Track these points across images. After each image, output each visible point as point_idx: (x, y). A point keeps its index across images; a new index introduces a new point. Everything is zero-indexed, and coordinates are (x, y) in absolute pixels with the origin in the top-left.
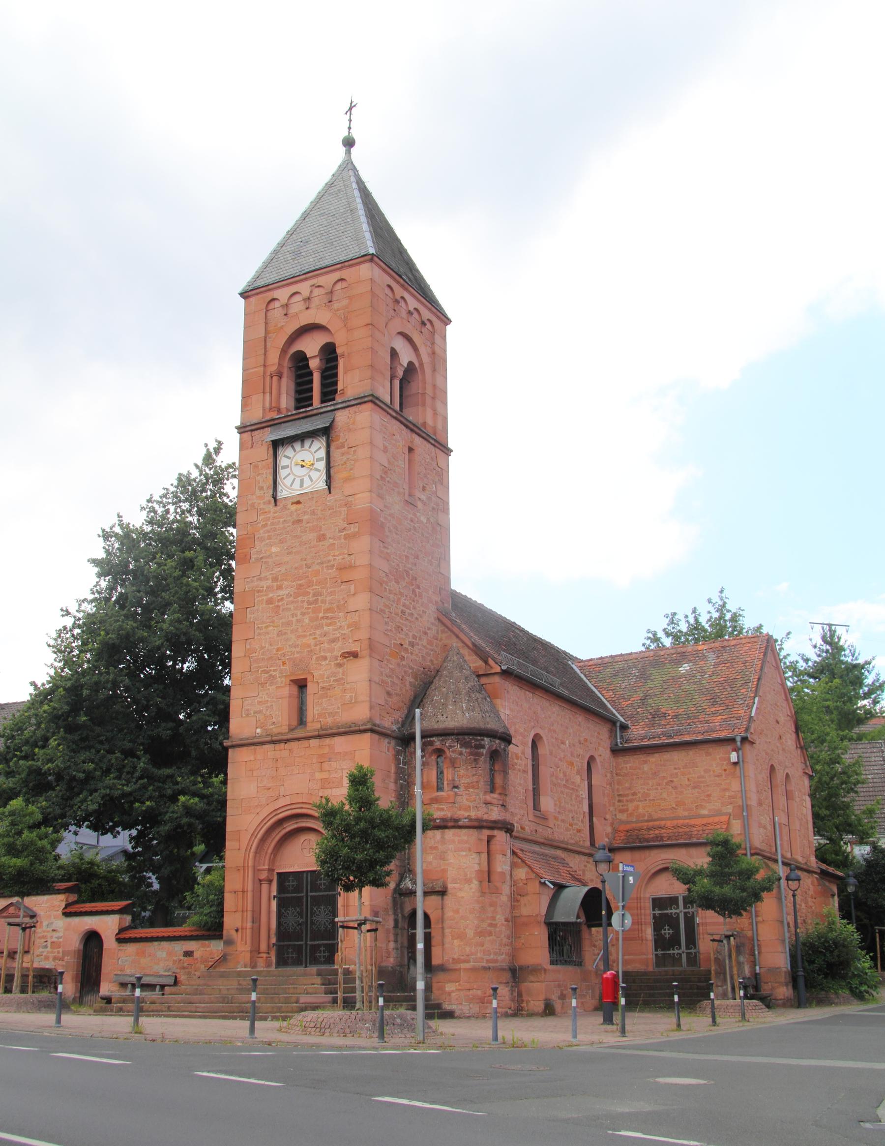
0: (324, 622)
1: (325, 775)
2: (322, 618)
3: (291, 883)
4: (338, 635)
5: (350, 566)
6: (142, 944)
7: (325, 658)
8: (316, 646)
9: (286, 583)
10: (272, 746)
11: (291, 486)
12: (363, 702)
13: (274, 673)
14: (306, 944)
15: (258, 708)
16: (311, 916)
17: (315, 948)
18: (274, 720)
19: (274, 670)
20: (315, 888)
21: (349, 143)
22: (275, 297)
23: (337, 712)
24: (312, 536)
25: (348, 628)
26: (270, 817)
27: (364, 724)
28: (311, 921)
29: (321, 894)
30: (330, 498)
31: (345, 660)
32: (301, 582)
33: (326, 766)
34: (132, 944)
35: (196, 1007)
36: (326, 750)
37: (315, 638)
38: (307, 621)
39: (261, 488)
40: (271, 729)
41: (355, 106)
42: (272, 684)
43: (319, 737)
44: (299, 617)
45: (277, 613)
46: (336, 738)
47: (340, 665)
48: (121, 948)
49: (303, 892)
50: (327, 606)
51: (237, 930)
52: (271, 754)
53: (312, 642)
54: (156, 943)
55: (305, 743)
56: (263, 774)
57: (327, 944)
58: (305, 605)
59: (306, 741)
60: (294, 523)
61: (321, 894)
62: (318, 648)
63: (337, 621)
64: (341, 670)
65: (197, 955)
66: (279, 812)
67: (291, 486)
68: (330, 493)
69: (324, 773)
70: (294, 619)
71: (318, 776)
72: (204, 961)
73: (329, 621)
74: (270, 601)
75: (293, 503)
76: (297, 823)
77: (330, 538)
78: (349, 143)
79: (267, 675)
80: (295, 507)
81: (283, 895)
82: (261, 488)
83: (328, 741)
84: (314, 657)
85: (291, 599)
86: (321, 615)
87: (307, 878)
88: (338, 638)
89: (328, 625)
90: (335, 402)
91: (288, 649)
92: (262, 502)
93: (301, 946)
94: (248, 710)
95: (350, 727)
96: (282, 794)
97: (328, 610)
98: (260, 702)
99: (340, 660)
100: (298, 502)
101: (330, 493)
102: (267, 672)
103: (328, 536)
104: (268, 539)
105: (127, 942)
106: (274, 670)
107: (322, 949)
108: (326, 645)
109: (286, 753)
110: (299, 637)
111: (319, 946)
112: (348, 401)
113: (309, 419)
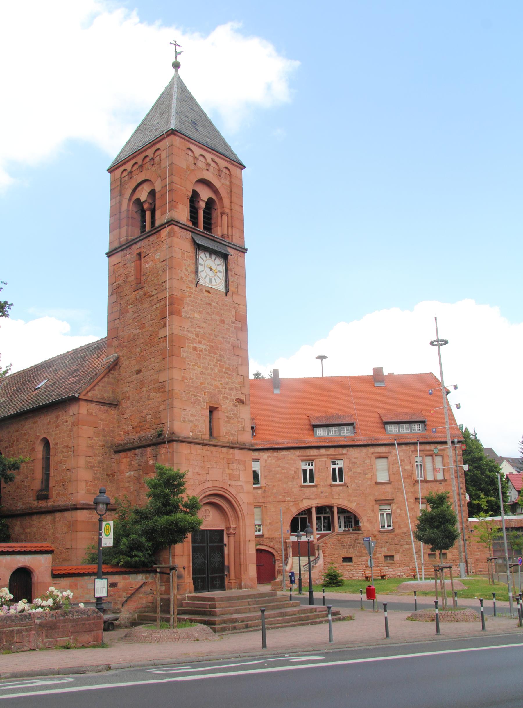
0: (226, 375)
1: (230, 472)
2: (225, 372)
3: (198, 537)
4: (233, 387)
5: (238, 347)
6: (74, 578)
7: (228, 399)
8: (222, 389)
9: (204, 341)
11: (216, 283)
12: (248, 432)
13: (200, 398)
14: (208, 576)
15: (191, 418)
16: (210, 559)
17: (213, 579)
18: (200, 429)
19: (200, 396)
20: (212, 541)
21: (176, 66)
23: (235, 434)
25: (238, 384)
26: (231, 496)
27: (248, 446)
28: (210, 561)
30: (225, 298)
31: (238, 403)
33: (231, 466)
34: (65, 579)
35: (278, 620)
36: (231, 457)
37: (221, 384)
38: (217, 371)
40: (199, 435)
41: (175, 42)
42: (198, 405)
43: (228, 447)
44: (212, 367)
45: (199, 358)
46: (235, 450)
47: (236, 406)
48: (55, 582)
49: (205, 543)
50: (227, 366)
51: (184, 568)
52: (200, 451)
53: (220, 386)
54: (86, 578)
55: (220, 449)
56: (196, 464)
57: (219, 576)
59: (220, 448)
60: (207, 304)
62: (223, 390)
63: (233, 377)
64: (236, 408)
65: (120, 585)
66: (228, 493)
67: (216, 283)
68: (226, 296)
69: (230, 470)
70: (209, 367)
72: (125, 590)
74: (195, 349)
75: (206, 291)
76: (209, 499)
77: (227, 324)
78: (176, 66)
79: (195, 398)
80: (206, 294)
81: (221, 544)
82: (187, 270)
83: (231, 451)
84: (222, 395)
85: (207, 353)
86: (224, 370)
87: (207, 533)
88: (234, 388)
89: (229, 378)
91: (207, 385)
93: (205, 577)
94: (184, 418)
95: (246, 445)
96: (208, 480)
97: (228, 369)
98: (192, 415)
99: (235, 402)
100: (209, 292)
101: (226, 296)
102: (195, 396)
103: (226, 322)
104: (192, 307)
105: (61, 577)
106: (200, 396)
107: (217, 579)
108: (227, 390)
109: (208, 453)
110: (213, 379)
111: (215, 577)
112: (236, 246)
113: (213, 242)
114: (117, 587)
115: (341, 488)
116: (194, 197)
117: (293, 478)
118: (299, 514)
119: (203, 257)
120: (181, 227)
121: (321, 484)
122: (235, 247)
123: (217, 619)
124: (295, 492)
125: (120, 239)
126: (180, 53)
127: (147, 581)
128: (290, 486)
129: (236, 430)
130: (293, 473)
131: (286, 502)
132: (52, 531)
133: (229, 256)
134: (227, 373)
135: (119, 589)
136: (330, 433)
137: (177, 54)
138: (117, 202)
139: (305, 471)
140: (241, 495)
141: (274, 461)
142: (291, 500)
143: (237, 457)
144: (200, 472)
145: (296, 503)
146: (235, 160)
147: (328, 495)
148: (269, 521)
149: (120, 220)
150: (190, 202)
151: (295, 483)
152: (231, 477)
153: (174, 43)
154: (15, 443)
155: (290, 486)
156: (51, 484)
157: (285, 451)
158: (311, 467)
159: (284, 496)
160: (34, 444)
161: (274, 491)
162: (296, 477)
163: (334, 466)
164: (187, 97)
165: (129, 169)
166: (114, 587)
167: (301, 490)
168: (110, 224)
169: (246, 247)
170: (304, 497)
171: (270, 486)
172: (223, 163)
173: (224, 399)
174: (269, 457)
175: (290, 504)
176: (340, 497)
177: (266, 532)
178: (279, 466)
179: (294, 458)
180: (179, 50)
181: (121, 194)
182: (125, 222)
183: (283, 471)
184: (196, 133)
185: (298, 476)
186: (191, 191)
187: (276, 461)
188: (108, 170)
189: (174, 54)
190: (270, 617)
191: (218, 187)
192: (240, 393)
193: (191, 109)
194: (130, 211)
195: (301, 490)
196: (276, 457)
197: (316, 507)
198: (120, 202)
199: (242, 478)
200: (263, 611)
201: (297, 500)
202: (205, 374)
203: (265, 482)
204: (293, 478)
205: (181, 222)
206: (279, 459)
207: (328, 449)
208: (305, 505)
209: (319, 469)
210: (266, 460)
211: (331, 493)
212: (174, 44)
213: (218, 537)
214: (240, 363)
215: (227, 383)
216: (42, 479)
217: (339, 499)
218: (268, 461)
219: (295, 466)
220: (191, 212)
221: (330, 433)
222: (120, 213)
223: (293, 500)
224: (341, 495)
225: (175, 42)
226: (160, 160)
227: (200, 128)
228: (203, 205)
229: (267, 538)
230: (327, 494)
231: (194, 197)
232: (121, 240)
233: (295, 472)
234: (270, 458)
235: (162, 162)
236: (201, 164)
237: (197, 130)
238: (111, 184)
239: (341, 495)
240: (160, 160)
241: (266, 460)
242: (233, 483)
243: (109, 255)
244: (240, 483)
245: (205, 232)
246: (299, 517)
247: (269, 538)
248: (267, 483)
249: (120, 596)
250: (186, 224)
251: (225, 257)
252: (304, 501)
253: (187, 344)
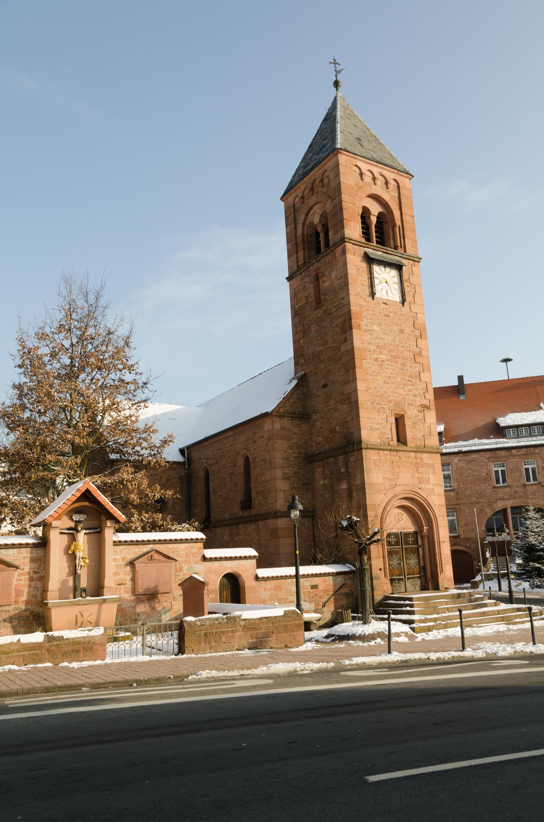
0: (409, 382)
3: (393, 540)
4: (417, 393)
12: (435, 436)
13: (385, 407)
15: (377, 426)
22: (358, 165)
24: (397, 328)
29: (410, 546)
31: (423, 409)
32: (393, 354)
38: (399, 379)
39: (362, 285)
43: (416, 452)
50: (409, 374)
58: (398, 369)
61: (410, 546)
63: (416, 384)
65: (321, 588)
68: (403, 306)
71: (417, 475)
74: (376, 360)
75: (383, 303)
79: (380, 406)
80: (384, 306)
82: (362, 285)
83: (419, 455)
85: (389, 362)
88: (417, 395)
90: (397, 251)
92: (364, 294)
96: (398, 484)
97: (409, 376)
100: (386, 304)
101: (403, 306)
103: (406, 332)
104: (371, 319)
109: (397, 459)
115: (535, 487)
116: (365, 214)
117: (486, 479)
118: (493, 515)
119: (376, 269)
120: (354, 244)
121: (515, 484)
122: (409, 257)
123: (415, 617)
124: (488, 494)
125: (298, 263)
126: (340, 72)
127: (346, 582)
128: (483, 488)
130: (485, 475)
131: (480, 504)
132: (257, 538)
133: (404, 267)
136: (521, 434)
137: (337, 72)
138: (293, 228)
139: (497, 472)
140: (432, 497)
141: (464, 464)
142: (485, 501)
143: (425, 461)
145: (490, 504)
146: (402, 170)
147: (522, 495)
148: (464, 522)
149: (296, 245)
150: (361, 219)
151: (487, 485)
152: (420, 481)
153: (333, 61)
154: (219, 460)
155: (483, 488)
156: (253, 495)
157: (475, 454)
158: (503, 468)
159: (477, 498)
160: (236, 459)
161: (467, 493)
162: (488, 479)
163: (527, 467)
164: (350, 114)
165: (300, 195)
166: (316, 589)
167: (495, 491)
168: (288, 250)
169: (420, 256)
170: (498, 497)
171: (462, 489)
172: (390, 175)
174: (459, 460)
175: (484, 506)
176: (535, 497)
177: (461, 533)
178: (470, 469)
179: (484, 460)
180: (339, 68)
181: (295, 221)
182: (301, 246)
183: (475, 474)
184: (361, 149)
185: (490, 478)
186: (362, 207)
187: (467, 464)
188: (281, 199)
189: (335, 73)
190: (469, 616)
191: (387, 201)
193: (355, 126)
194: (305, 236)
195: (495, 491)
196: (467, 460)
197: (511, 507)
198: (296, 228)
199: (432, 481)
200: (460, 611)
201: (490, 501)
202: (388, 383)
203: (457, 485)
204: (486, 479)
205: (354, 239)
206: (470, 462)
207: (519, 450)
208: (500, 505)
209: (511, 470)
210: (457, 464)
211: (525, 493)
212: (333, 63)
213: (412, 539)
215: (411, 391)
216: (245, 491)
217: (535, 498)
218: (459, 465)
219: (486, 468)
220: (363, 228)
221: (521, 434)
222: (296, 238)
223: (487, 501)
224: (536, 494)
225: (335, 61)
226: (329, 182)
227: (365, 144)
228: (374, 220)
229: (463, 539)
230: (522, 494)
231: (365, 214)
232: (299, 264)
233: (487, 474)
234: (461, 462)
235: (331, 182)
236: (368, 177)
237: (362, 146)
238: (286, 211)
239: (536, 494)
240: (329, 182)
241: (457, 464)
242: (423, 486)
243: (289, 279)
244: (430, 486)
245: (378, 246)
246: (494, 518)
247: (465, 539)
248: (459, 486)
249: (321, 597)
250: (358, 240)
251: (399, 267)
252: (498, 502)
253: (368, 356)
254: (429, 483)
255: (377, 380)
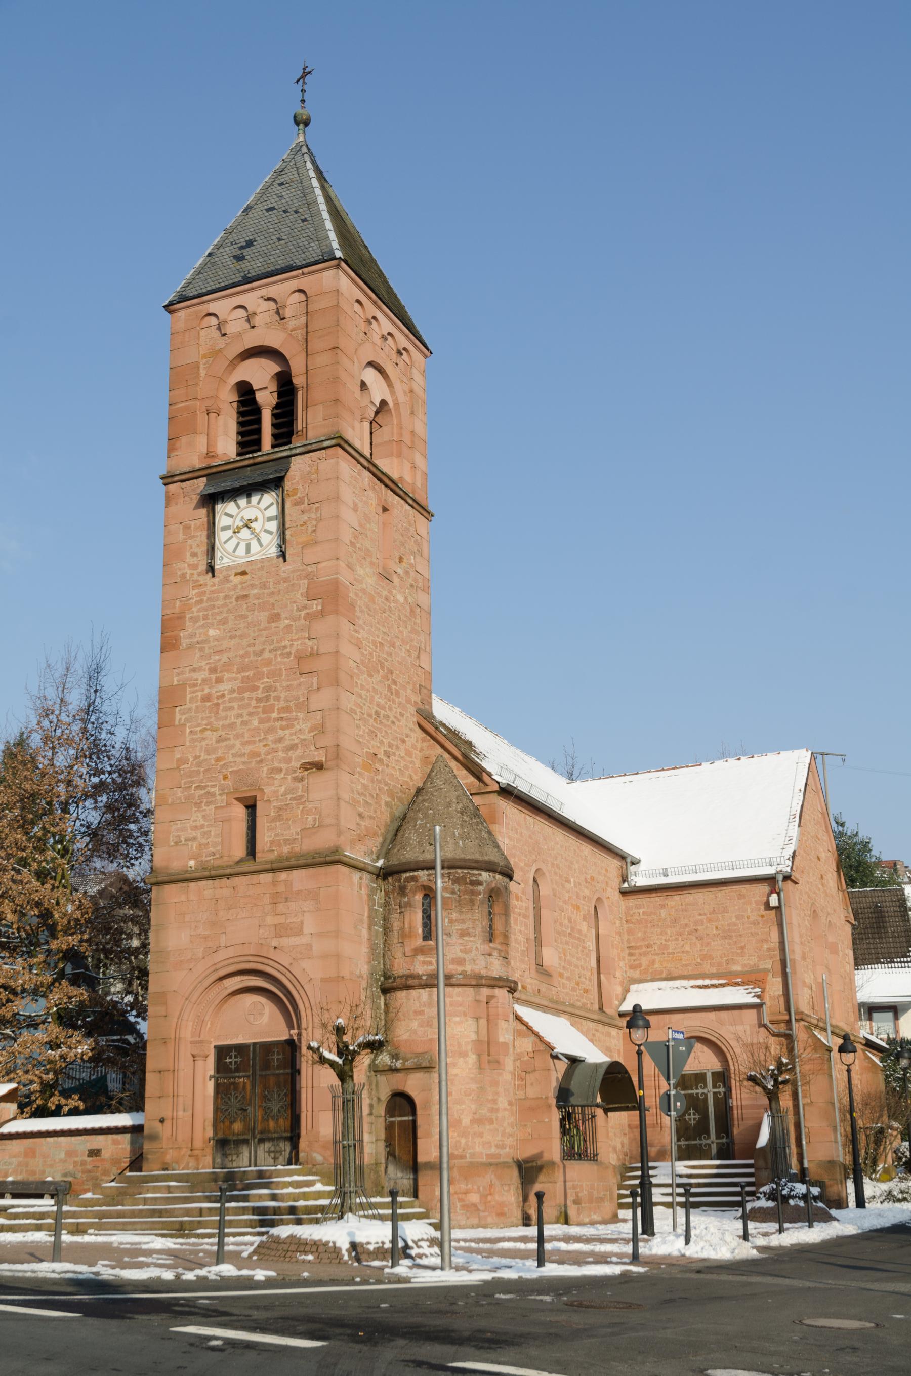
0: (278, 724)
1: (280, 920)
4: (296, 741)
9: (227, 676)
10: (210, 882)
13: (212, 790)
22: (211, 312)
23: (295, 839)
24: (263, 616)
25: (309, 732)
31: (306, 773)
32: (247, 674)
33: (281, 907)
38: (255, 723)
39: (194, 555)
41: (309, 73)
42: (208, 804)
43: (273, 870)
46: (295, 872)
50: (282, 704)
51: (162, 1121)
52: (208, 893)
58: (254, 703)
62: (269, 757)
63: (295, 723)
64: (300, 785)
65: (106, 1154)
68: (285, 561)
71: (270, 920)
73: (284, 723)
75: (236, 574)
79: (203, 792)
80: (239, 578)
82: (194, 555)
83: (283, 876)
85: (235, 695)
86: (274, 715)
88: (296, 744)
89: (283, 728)
90: (292, 446)
91: (231, 759)
92: (195, 572)
99: (298, 774)
100: (244, 573)
103: (283, 615)
104: (204, 619)
106: (212, 786)
108: (281, 754)
109: (226, 892)
110: (244, 744)
114: (100, 1156)
120: (182, 481)
129: (299, 830)
134: (282, 718)
135: (103, 1160)
140: (306, 964)
143: (297, 886)
144: (206, 933)
152: (282, 930)
173: (271, 773)
192: (313, 748)
199: (307, 929)
202: (226, 739)
214: (315, 686)
215: (280, 740)
242: (286, 942)
253: (188, 696)
254: (299, 931)
255: (204, 739)
